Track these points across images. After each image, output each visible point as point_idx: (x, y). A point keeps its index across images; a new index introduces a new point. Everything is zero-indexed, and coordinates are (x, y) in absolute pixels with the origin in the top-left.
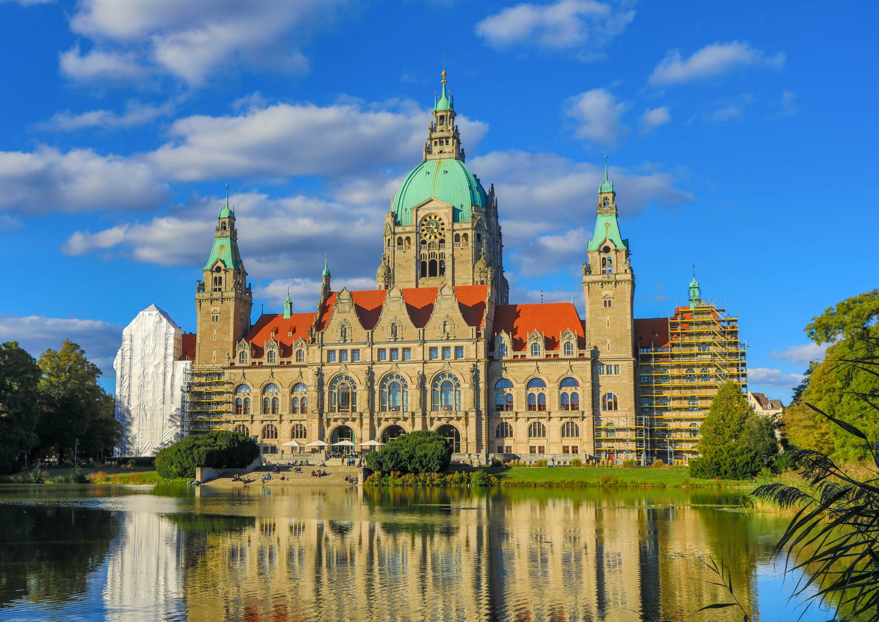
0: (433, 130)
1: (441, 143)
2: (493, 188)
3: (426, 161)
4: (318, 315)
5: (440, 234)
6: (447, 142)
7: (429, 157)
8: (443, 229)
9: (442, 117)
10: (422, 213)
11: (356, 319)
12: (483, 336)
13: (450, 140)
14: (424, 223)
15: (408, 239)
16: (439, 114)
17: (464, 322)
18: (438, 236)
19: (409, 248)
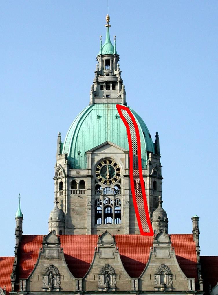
0: (99, 73)
1: (108, 88)
2: (157, 136)
3: (94, 104)
4: (16, 259)
5: (115, 180)
6: (114, 88)
7: (96, 100)
8: (118, 175)
9: (108, 63)
10: (97, 158)
11: (65, 265)
12: (202, 289)
13: (118, 87)
14: (100, 168)
15: (82, 183)
16: (105, 58)
17: (182, 273)
18: (113, 181)
19: (84, 192)
